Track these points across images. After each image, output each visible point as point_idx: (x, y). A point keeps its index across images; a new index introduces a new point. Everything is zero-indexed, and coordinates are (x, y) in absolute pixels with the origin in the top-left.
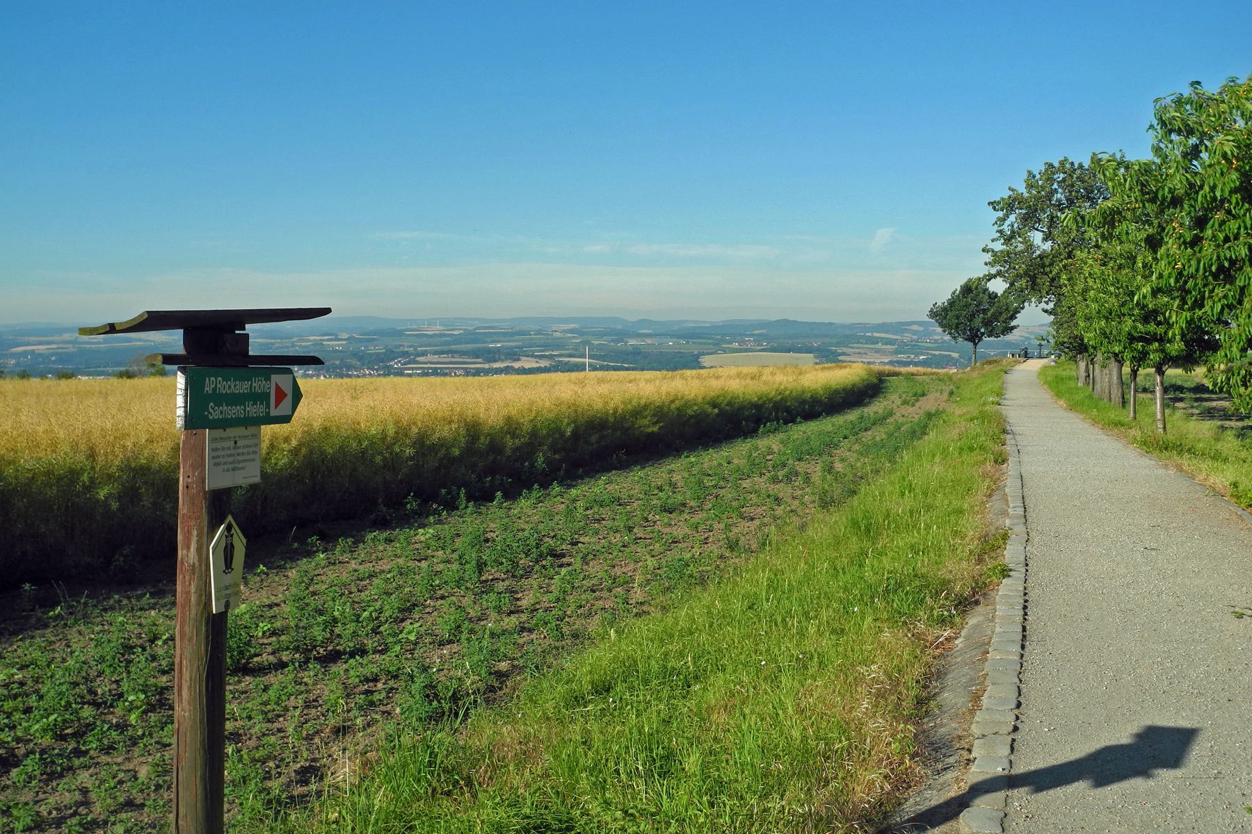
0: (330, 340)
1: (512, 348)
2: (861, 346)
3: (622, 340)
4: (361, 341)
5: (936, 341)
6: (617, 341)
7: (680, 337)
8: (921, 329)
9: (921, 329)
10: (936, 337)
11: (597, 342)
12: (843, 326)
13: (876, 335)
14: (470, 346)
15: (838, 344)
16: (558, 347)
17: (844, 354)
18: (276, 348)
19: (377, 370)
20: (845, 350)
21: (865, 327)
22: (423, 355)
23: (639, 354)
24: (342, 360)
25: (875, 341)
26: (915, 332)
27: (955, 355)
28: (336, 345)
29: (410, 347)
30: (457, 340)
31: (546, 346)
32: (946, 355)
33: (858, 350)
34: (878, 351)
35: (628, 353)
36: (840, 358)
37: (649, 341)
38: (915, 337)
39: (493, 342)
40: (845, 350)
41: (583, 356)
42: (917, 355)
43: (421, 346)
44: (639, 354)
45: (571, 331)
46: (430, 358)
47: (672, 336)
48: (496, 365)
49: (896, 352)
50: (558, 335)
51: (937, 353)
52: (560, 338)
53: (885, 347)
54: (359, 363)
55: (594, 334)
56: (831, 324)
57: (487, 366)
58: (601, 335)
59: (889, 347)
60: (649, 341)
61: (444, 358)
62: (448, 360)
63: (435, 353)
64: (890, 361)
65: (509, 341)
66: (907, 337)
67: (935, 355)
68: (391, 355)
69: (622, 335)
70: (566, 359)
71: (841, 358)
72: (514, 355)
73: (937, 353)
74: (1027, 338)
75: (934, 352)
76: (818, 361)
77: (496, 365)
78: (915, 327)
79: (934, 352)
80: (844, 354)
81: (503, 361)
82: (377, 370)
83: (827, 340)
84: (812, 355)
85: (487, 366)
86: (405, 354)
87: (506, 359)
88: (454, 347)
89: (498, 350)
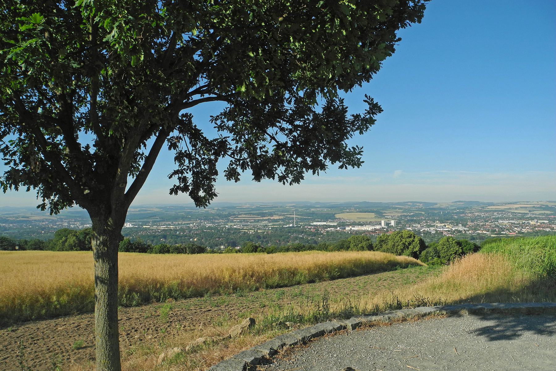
0: (211, 210)
1: (271, 212)
3: (309, 209)
4: (221, 210)
5: (417, 208)
6: (307, 209)
7: (328, 208)
8: (411, 204)
9: (411, 204)
11: (300, 210)
12: (385, 204)
13: (396, 206)
14: (257, 212)
15: (383, 210)
16: (287, 212)
18: (193, 213)
19: (224, 220)
20: (385, 211)
21: (393, 204)
22: (240, 215)
23: (314, 214)
24: (213, 217)
25: (396, 208)
26: (409, 205)
27: (423, 213)
28: (213, 212)
29: (237, 212)
30: (253, 210)
31: (283, 211)
34: (396, 212)
35: (311, 213)
36: (383, 214)
37: (318, 209)
39: (265, 210)
40: (385, 211)
42: (410, 213)
43: (241, 212)
44: (314, 214)
45: (292, 206)
46: (243, 216)
47: (326, 207)
48: (265, 218)
49: (403, 212)
50: (288, 207)
51: (417, 212)
52: (288, 209)
53: (399, 210)
54: (219, 218)
55: (300, 207)
57: (262, 218)
58: (302, 207)
59: (400, 210)
60: (318, 209)
61: (247, 216)
62: (249, 216)
63: (245, 214)
65: (271, 210)
66: (407, 207)
67: (416, 213)
68: (230, 215)
69: (309, 207)
70: (289, 216)
71: (383, 214)
72: (271, 215)
73: (417, 212)
76: (376, 215)
77: (265, 218)
78: (409, 204)
80: (385, 213)
81: (267, 216)
82: (224, 220)
83: (379, 208)
85: (262, 218)
86: (234, 214)
87: (269, 216)
89: (266, 213)
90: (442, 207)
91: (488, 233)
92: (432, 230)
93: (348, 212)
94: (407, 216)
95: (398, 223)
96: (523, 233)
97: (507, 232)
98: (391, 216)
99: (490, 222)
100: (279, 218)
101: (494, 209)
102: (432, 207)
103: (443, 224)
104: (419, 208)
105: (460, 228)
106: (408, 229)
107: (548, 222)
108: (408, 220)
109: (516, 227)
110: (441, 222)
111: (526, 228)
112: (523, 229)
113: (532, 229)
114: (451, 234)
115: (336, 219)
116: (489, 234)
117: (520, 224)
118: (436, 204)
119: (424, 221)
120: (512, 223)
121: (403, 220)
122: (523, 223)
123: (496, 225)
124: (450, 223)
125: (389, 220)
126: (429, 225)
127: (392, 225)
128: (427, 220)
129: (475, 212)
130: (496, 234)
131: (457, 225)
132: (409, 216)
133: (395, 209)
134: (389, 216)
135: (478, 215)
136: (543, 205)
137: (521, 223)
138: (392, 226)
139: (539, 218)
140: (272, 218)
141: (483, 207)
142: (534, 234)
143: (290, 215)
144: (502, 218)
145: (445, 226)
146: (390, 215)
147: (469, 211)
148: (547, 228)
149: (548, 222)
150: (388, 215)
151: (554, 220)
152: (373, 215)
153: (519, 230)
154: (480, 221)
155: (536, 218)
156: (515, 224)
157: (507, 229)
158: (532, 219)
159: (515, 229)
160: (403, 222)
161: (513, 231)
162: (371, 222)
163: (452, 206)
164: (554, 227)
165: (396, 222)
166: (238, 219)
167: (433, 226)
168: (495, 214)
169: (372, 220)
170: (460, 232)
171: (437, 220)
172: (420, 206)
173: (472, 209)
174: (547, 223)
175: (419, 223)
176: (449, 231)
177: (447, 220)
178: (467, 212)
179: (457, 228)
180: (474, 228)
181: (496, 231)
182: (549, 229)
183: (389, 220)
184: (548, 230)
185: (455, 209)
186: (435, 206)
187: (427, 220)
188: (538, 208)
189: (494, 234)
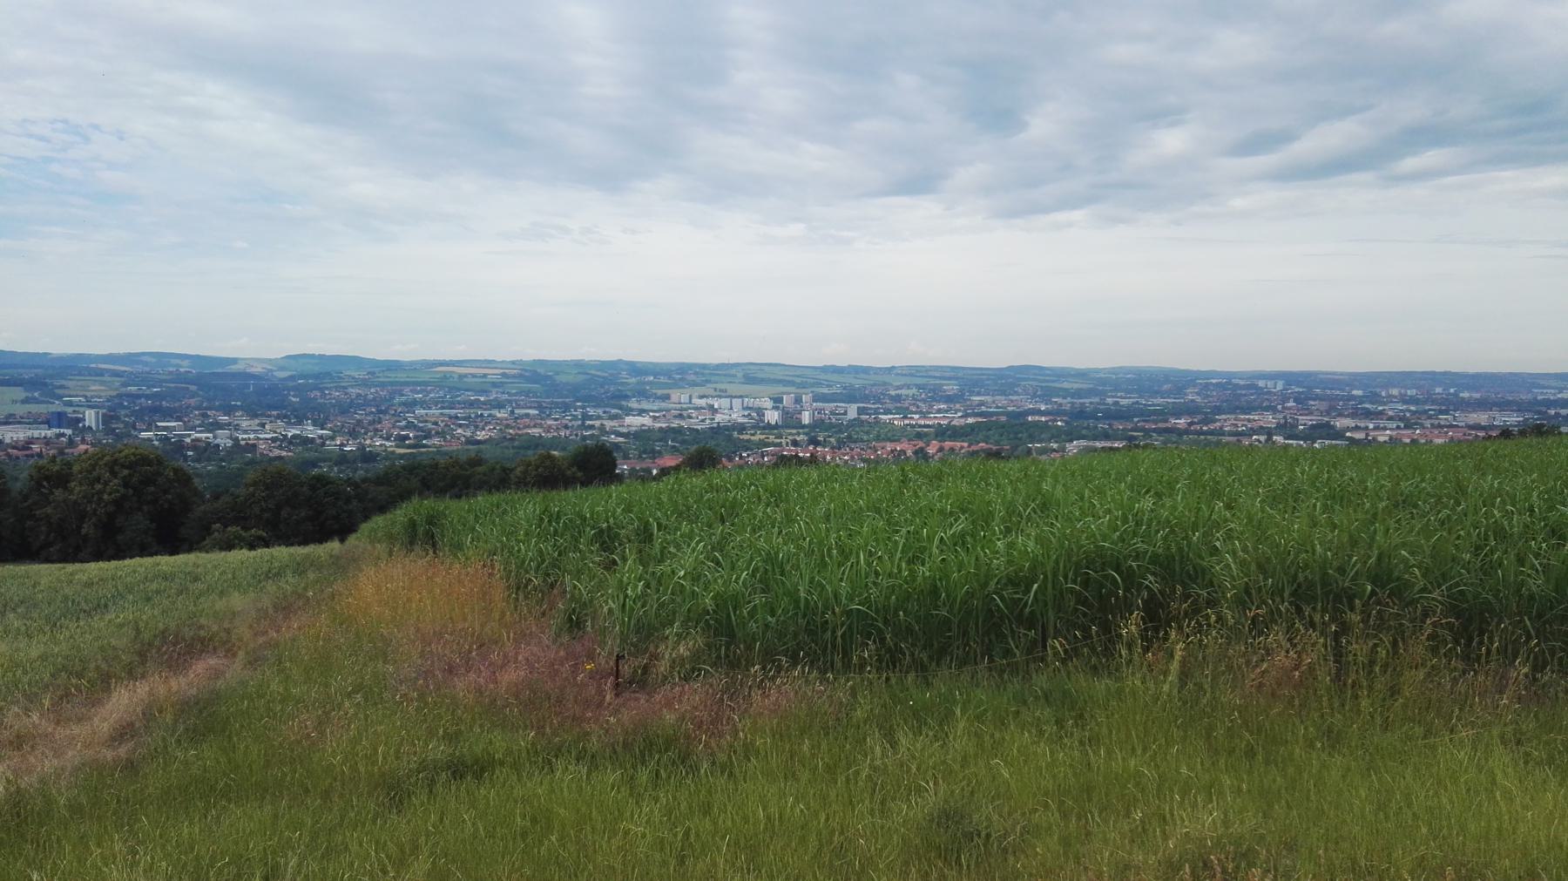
2: (83, 378)
5: (171, 373)
8: (154, 360)
9: (154, 360)
10: (171, 369)
12: (61, 358)
17: (62, 387)
20: (63, 382)
25: (101, 373)
32: (183, 389)
33: (79, 383)
38: (147, 369)
42: (148, 388)
51: (172, 385)
56: (46, 354)
64: (118, 394)
67: (169, 387)
73: (172, 385)
74: (271, 371)
75: (168, 385)
79: (168, 385)
90: (253, 370)
91: (388, 444)
92: (223, 439)
94: (138, 397)
95: (107, 420)
96: (479, 442)
97: (436, 441)
98: (86, 397)
99: (393, 415)
101: (402, 380)
102: (220, 370)
103: (257, 421)
104: (180, 373)
105: (311, 431)
106: (144, 435)
107: (537, 412)
108: (142, 409)
109: (460, 426)
110: (254, 415)
111: (487, 428)
112: (478, 433)
113: (501, 429)
114: (280, 448)
116: (391, 446)
117: (470, 417)
118: (234, 361)
119: (197, 412)
120: (450, 417)
121: (125, 407)
122: (477, 416)
123: (409, 422)
124: (278, 417)
125: (77, 409)
126: (212, 424)
127: (87, 424)
128: (207, 408)
129: (352, 387)
130: (409, 447)
131: (300, 423)
132: (147, 397)
133: (97, 375)
134: (77, 396)
135: (359, 395)
136: (526, 371)
137: (473, 416)
138: (90, 428)
139: (516, 401)
141: (374, 373)
142: (506, 444)
144: (424, 404)
145: (263, 425)
146: (82, 393)
147: (333, 382)
148: (535, 426)
149: (537, 412)
150: (72, 393)
151: (551, 408)
152: (20, 393)
153: (468, 434)
154: (364, 410)
155: (510, 402)
156: (457, 418)
157: (437, 433)
158: (500, 406)
159: (459, 431)
160: (126, 416)
161: (453, 436)
162: (11, 415)
163: (282, 369)
164: (550, 427)
165: (104, 415)
167: (221, 426)
168: (407, 390)
169: (20, 410)
170: (306, 441)
171: (236, 408)
172: (182, 367)
173: (341, 378)
174: (534, 415)
175: (179, 419)
176: (274, 440)
177: (271, 407)
178: (329, 386)
179: (299, 432)
180: (349, 431)
181: (410, 438)
182: (541, 430)
183: (77, 409)
184: (535, 431)
185: (292, 378)
186: (234, 368)
187: (207, 408)
188: (514, 376)
189: (403, 447)
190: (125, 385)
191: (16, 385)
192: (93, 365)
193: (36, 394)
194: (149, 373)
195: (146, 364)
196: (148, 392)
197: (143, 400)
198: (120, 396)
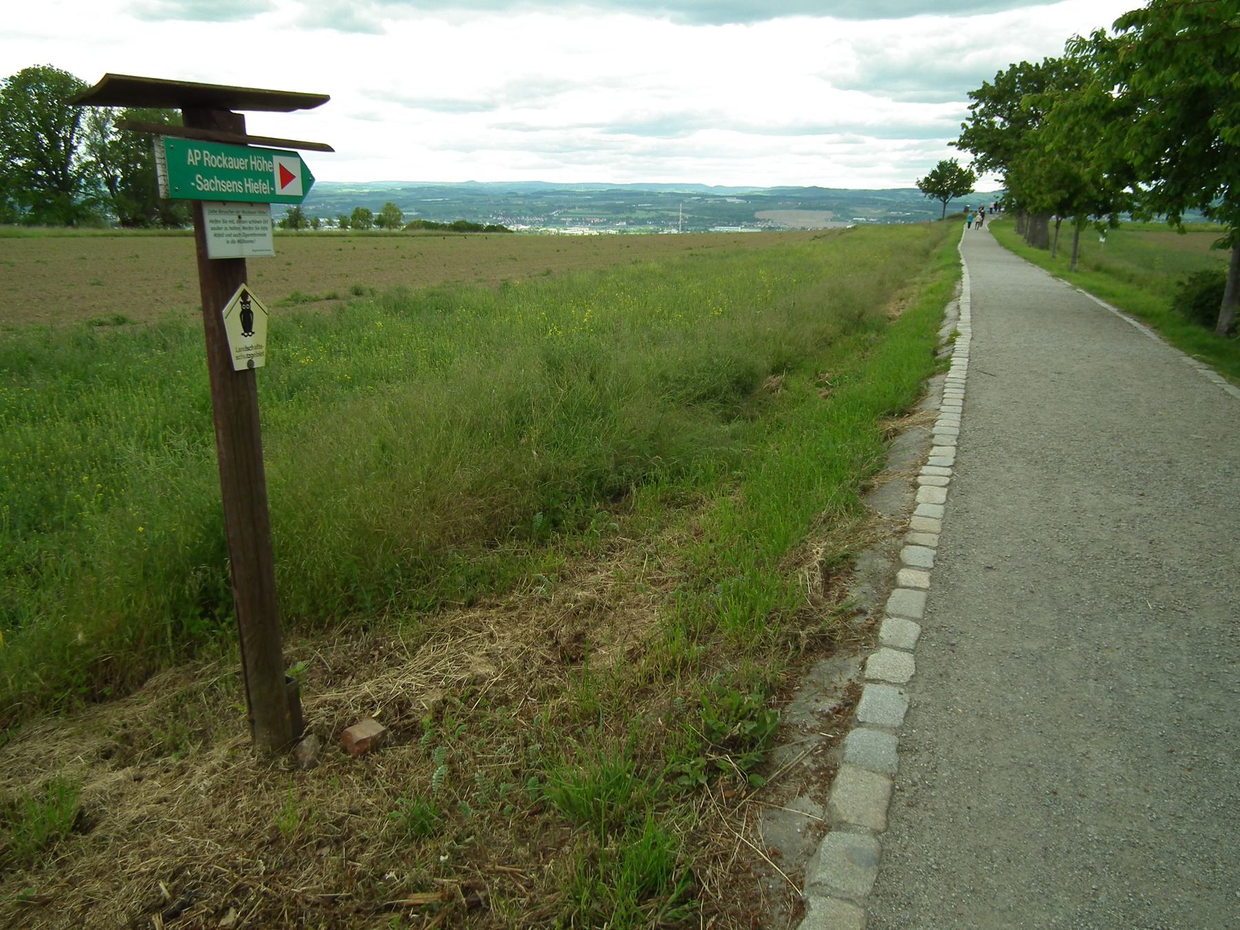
8: (908, 194)
9: (908, 194)
17: (853, 211)
38: (903, 200)
39: (618, 200)
41: (678, 211)
42: (904, 212)
61: (585, 210)
70: (666, 212)
84: (830, 212)
88: (593, 203)
93: (781, 208)
100: (647, 216)
115: (758, 220)
132: (903, 219)
140: (634, 216)
143: (669, 210)
152: (829, 214)
166: (569, 217)
190: (890, 211)
191: (828, 209)
192: (872, 197)
193: (839, 216)
194: (904, 202)
195: (903, 196)
196: (903, 215)
197: (899, 221)
198: (886, 218)
